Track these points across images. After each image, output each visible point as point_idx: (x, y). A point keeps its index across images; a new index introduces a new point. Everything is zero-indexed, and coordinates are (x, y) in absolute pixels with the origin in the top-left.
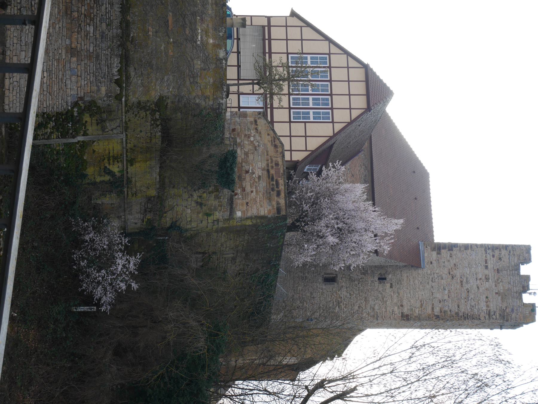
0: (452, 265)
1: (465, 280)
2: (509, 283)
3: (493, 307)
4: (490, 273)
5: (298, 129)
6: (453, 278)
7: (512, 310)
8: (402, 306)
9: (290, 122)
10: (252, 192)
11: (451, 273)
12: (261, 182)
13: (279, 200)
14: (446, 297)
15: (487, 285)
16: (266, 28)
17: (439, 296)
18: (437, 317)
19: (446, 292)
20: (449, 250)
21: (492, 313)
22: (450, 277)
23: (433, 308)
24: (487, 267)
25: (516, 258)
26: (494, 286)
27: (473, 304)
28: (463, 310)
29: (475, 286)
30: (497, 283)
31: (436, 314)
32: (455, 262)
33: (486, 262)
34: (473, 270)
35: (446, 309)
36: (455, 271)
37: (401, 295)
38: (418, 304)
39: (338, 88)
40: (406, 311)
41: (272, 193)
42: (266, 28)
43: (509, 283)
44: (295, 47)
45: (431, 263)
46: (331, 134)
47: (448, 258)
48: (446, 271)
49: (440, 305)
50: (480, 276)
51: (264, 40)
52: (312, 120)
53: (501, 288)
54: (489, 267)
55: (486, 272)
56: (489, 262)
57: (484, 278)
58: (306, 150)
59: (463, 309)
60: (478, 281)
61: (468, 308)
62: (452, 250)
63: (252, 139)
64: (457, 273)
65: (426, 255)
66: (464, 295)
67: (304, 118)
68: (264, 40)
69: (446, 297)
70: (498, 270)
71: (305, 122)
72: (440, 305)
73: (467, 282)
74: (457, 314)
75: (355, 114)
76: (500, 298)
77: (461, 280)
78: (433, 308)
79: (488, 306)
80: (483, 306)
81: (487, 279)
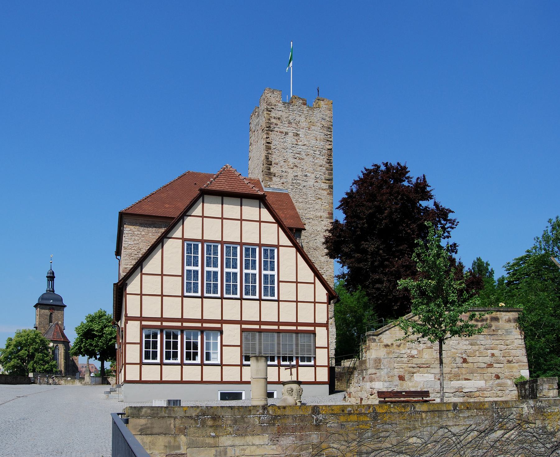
0: (285, 164)
4: (291, 131)
5: (287, 291)
6: (296, 166)
10: (493, 355)
11: (292, 166)
12: (478, 342)
13: (504, 319)
14: (313, 176)
16: (144, 323)
18: (331, 187)
20: (271, 165)
22: (295, 168)
24: (287, 133)
25: (279, 104)
28: (324, 163)
29: (304, 147)
31: (327, 187)
33: (282, 132)
35: (323, 177)
36: (290, 163)
37: (312, 217)
39: (232, 234)
40: (325, 215)
41: (493, 328)
42: (144, 323)
44: (174, 286)
45: (283, 183)
46: (294, 249)
48: (290, 171)
52: (275, 273)
54: (286, 131)
55: (291, 134)
57: (296, 138)
58: (314, 283)
60: (299, 143)
62: (271, 162)
63: (414, 352)
67: (273, 282)
70: (289, 123)
71: (279, 282)
75: (266, 215)
76: (313, 128)
77: (298, 158)
81: (297, 135)
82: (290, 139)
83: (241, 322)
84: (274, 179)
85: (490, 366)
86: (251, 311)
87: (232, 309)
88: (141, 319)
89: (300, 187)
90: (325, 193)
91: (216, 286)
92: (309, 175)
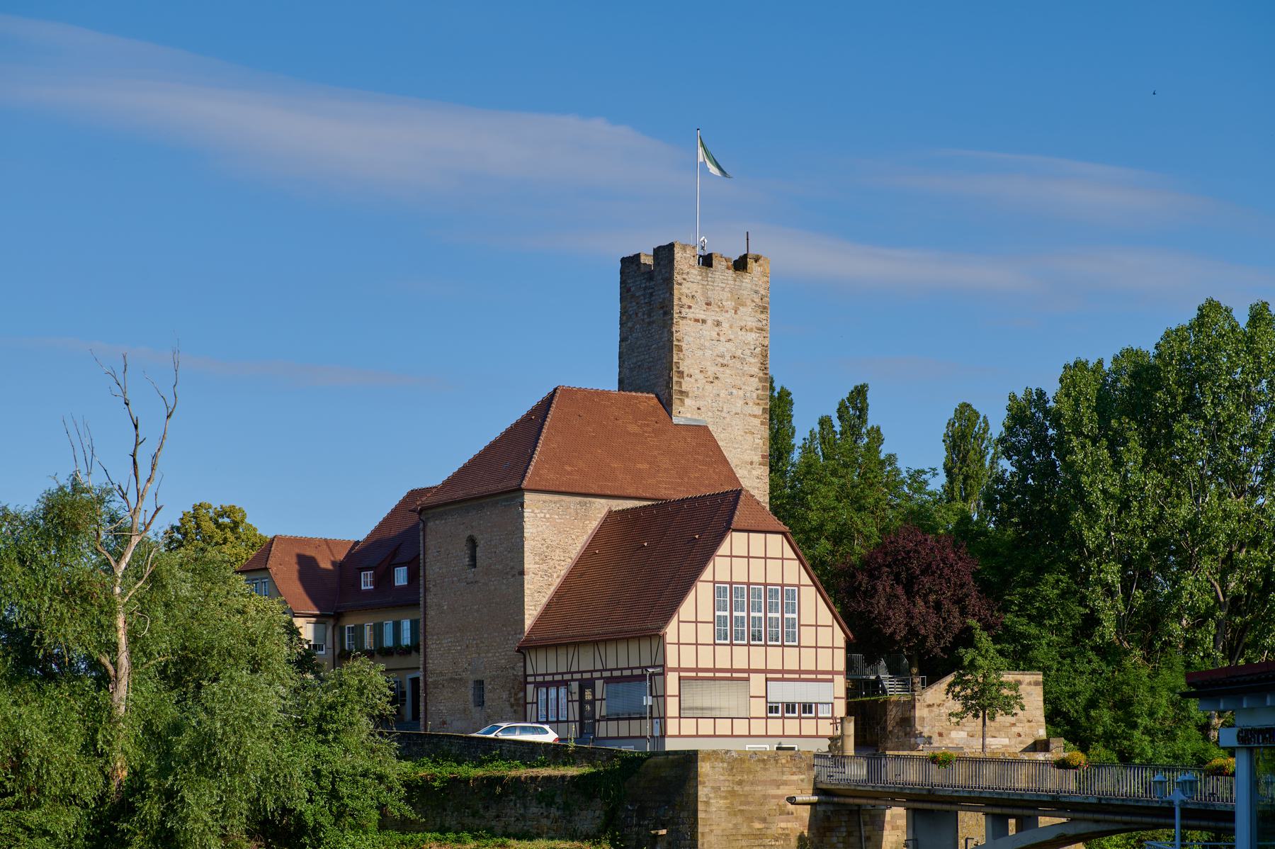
1: (720, 360)
2: (723, 289)
3: (751, 322)
4: (711, 317)
5: (807, 636)
7: (756, 292)
8: (752, 463)
9: (799, 646)
15: (725, 325)
17: (740, 403)
19: (734, 391)
21: (760, 325)
23: (755, 416)
24: (704, 321)
26: (728, 315)
27: (748, 352)
29: (728, 345)
30: (722, 308)
32: (697, 371)
34: (707, 344)
35: (755, 395)
38: (749, 437)
42: (682, 674)
43: (723, 289)
44: (706, 633)
47: (692, 380)
48: (709, 387)
49: (751, 404)
50: (714, 334)
51: (697, 678)
53: (729, 304)
55: (709, 322)
56: (698, 316)
59: (755, 370)
61: (752, 360)
64: (712, 369)
65: (689, 416)
66: (739, 365)
68: (732, 679)
69: (741, 393)
72: (751, 404)
73: (722, 356)
74: (761, 380)
78: (755, 416)
79: (751, 330)
80: (752, 337)
81: (718, 324)
82: (709, 331)
83: (765, 671)
84: (688, 401)
85: (1014, 725)
86: (775, 658)
87: (757, 657)
88: (679, 669)
89: (724, 414)
90: (757, 422)
91: (743, 632)
92: (734, 391)
